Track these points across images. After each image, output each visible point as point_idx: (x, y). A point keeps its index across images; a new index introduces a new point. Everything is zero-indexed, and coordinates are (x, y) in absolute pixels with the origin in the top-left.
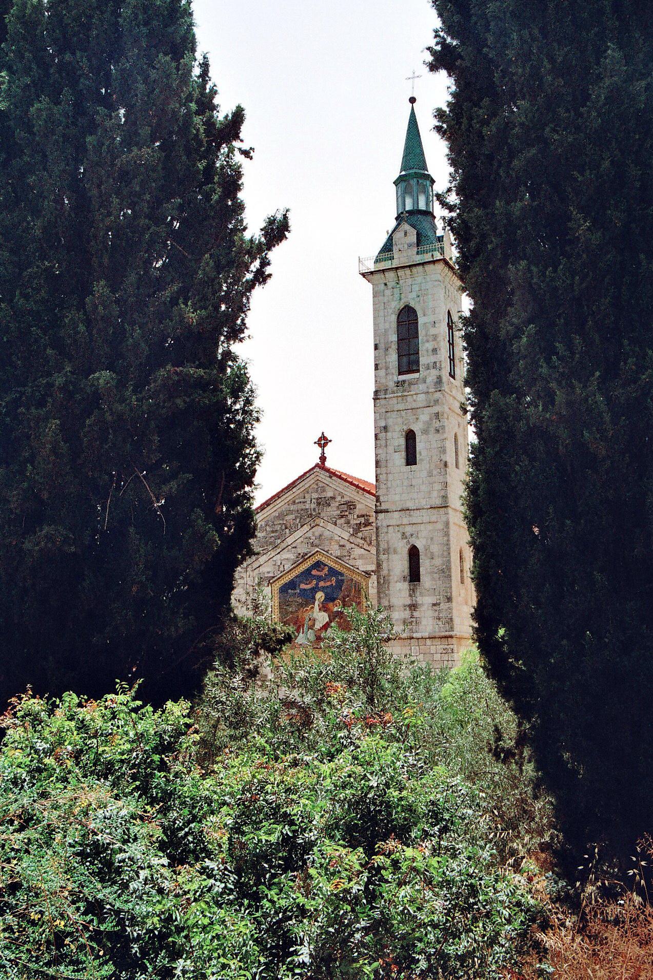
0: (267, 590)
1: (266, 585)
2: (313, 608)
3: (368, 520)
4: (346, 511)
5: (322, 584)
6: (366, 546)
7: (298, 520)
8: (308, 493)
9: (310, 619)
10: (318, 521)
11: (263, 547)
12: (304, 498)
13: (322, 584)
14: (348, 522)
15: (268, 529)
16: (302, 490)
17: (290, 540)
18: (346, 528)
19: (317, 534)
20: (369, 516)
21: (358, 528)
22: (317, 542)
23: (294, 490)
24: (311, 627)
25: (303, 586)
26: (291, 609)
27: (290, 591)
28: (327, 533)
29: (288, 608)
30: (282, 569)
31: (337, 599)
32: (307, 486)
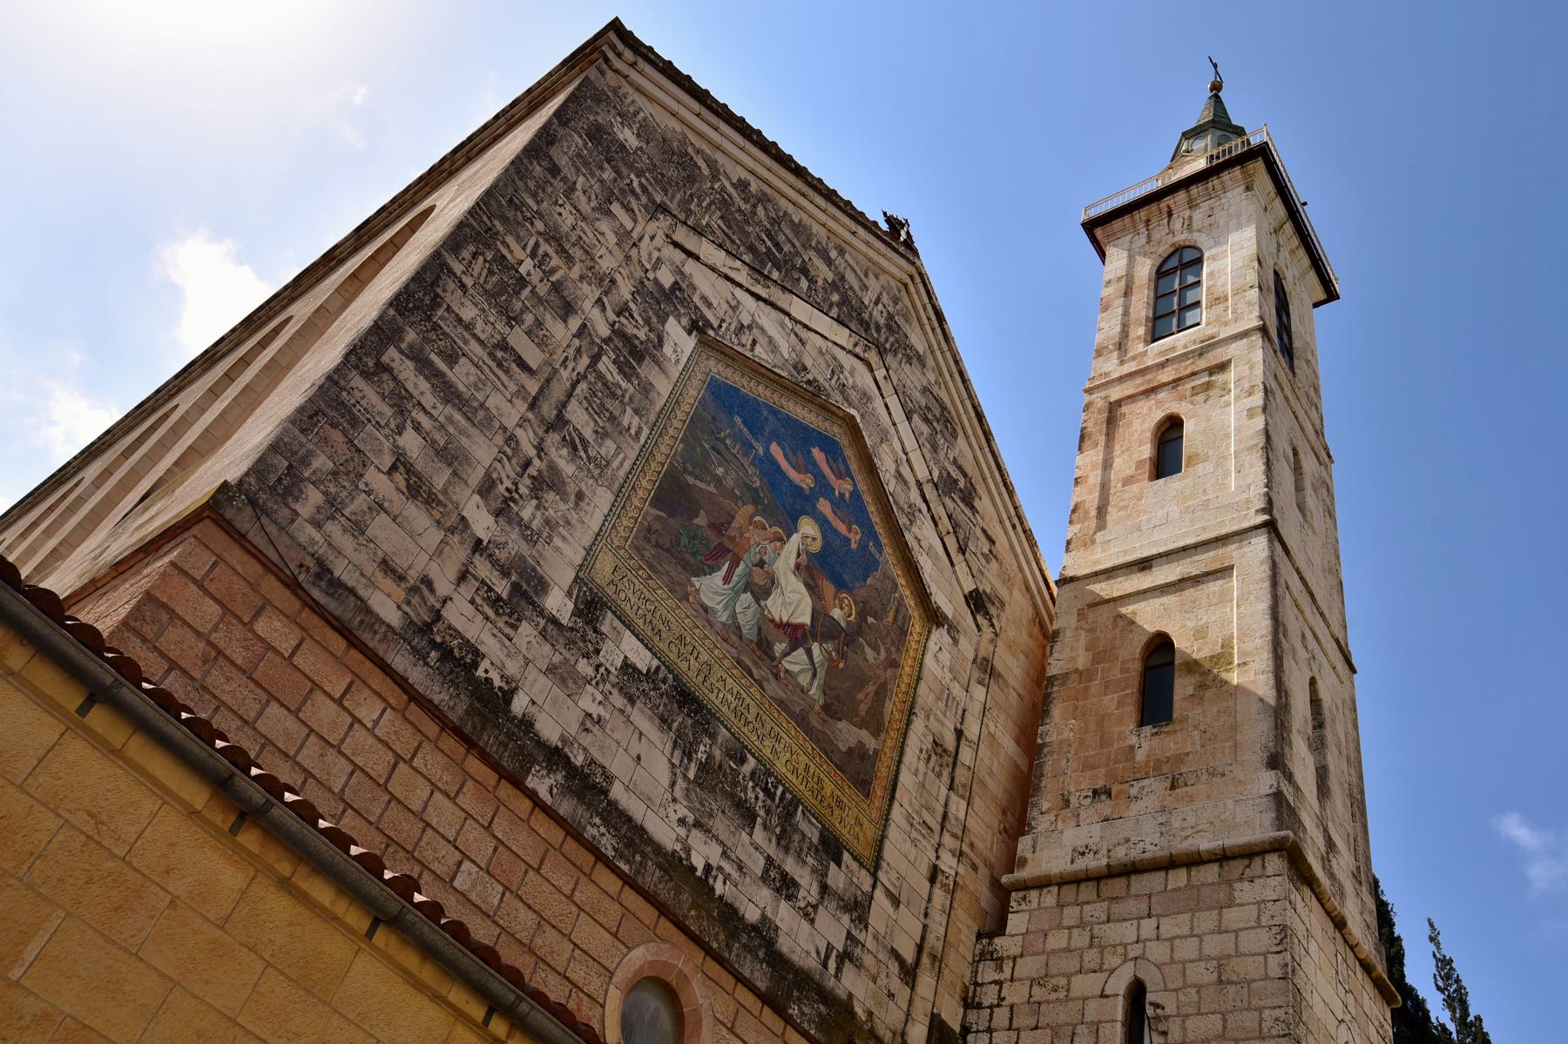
0: (679, 341)
1: (685, 321)
2: (783, 542)
3: (970, 494)
4: (938, 421)
5: (824, 506)
6: (951, 542)
7: (835, 298)
8: (877, 277)
9: (761, 564)
10: (872, 356)
11: (729, 227)
12: (866, 275)
13: (824, 506)
14: (935, 448)
15: (760, 211)
16: (871, 254)
17: (800, 309)
18: (928, 456)
19: (859, 383)
20: (975, 489)
21: (946, 485)
22: (853, 395)
23: (861, 232)
24: (761, 593)
25: (775, 450)
26: (720, 471)
27: (738, 420)
28: (878, 403)
29: (713, 454)
30: (746, 339)
31: (850, 591)
32: (885, 263)
